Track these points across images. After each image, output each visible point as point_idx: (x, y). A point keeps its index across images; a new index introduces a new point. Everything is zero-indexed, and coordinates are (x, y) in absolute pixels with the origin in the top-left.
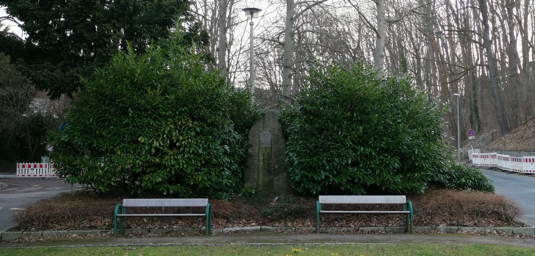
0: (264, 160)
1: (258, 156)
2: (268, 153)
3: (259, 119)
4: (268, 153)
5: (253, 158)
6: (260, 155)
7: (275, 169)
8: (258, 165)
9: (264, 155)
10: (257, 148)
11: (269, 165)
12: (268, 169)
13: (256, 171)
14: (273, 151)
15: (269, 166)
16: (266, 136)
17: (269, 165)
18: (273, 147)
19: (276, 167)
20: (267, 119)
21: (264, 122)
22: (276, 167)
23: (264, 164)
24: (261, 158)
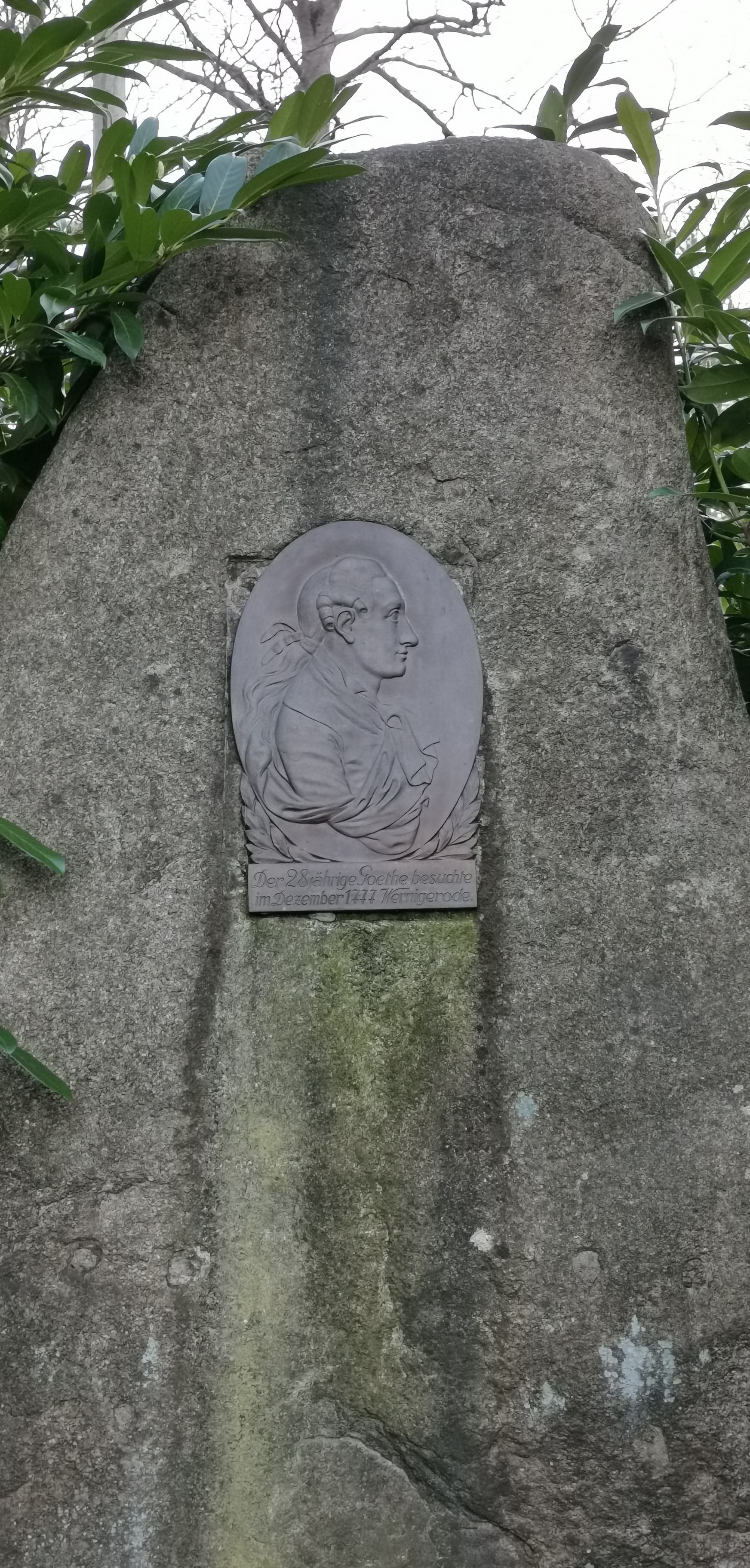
0: (321, 1199)
1: (195, 1098)
2: (428, 1028)
3: (228, 287)
4: (428, 1028)
5: (74, 1152)
6: (236, 1079)
7: (586, 1424)
8: (188, 1315)
9: (319, 1081)
10: (170, 909)
11: (447, 1313)
12: (416, 1409)
13: (144, 1464)
14: (529, 976)
15: (449, 1354)
16: (374, 643)
17: (447, 1313)
18: (526, 903)
19: (632, 1366)
20: (377, 307)
21: (326, 351)
22: (632, 1366)
23: (327, 1288)
24: (262, 1146)
